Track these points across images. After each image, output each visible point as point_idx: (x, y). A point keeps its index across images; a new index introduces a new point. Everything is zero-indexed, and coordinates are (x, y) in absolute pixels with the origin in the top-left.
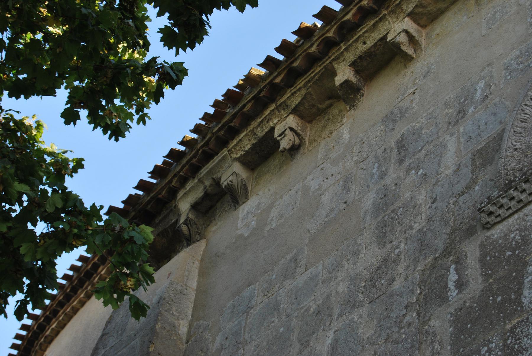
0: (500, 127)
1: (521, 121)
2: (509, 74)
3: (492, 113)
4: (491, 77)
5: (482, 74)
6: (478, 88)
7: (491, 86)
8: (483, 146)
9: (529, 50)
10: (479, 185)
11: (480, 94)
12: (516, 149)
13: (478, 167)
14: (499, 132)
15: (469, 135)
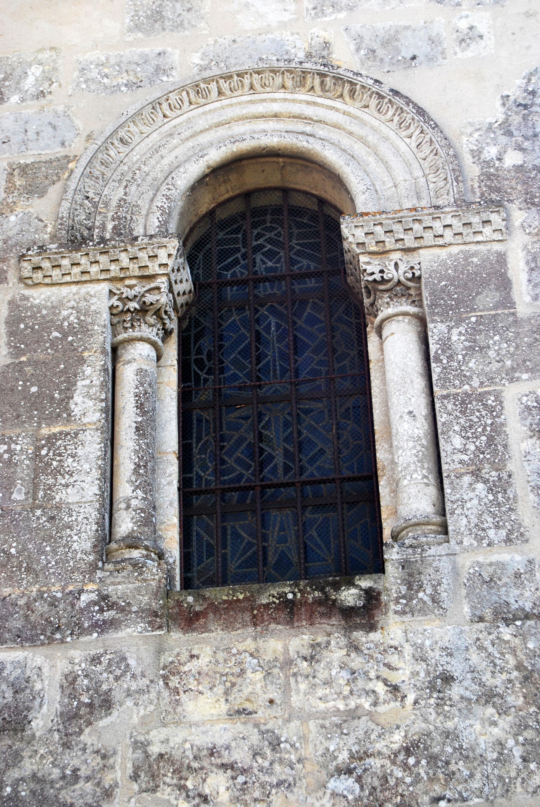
0: (60, 149)
1: (101, 162)
2: (86, 82)
3: (50, 123)
4: (53, 69)
5: (40, 56)
6: (29, 73)
7: (53, 83)
8: (28, 162)
9: (122, 65)
10: (17, 216)
11: (33, 83)
12: (88, 198)
13: (19, 189)
14: (58, 155)
15: (8, 134)
